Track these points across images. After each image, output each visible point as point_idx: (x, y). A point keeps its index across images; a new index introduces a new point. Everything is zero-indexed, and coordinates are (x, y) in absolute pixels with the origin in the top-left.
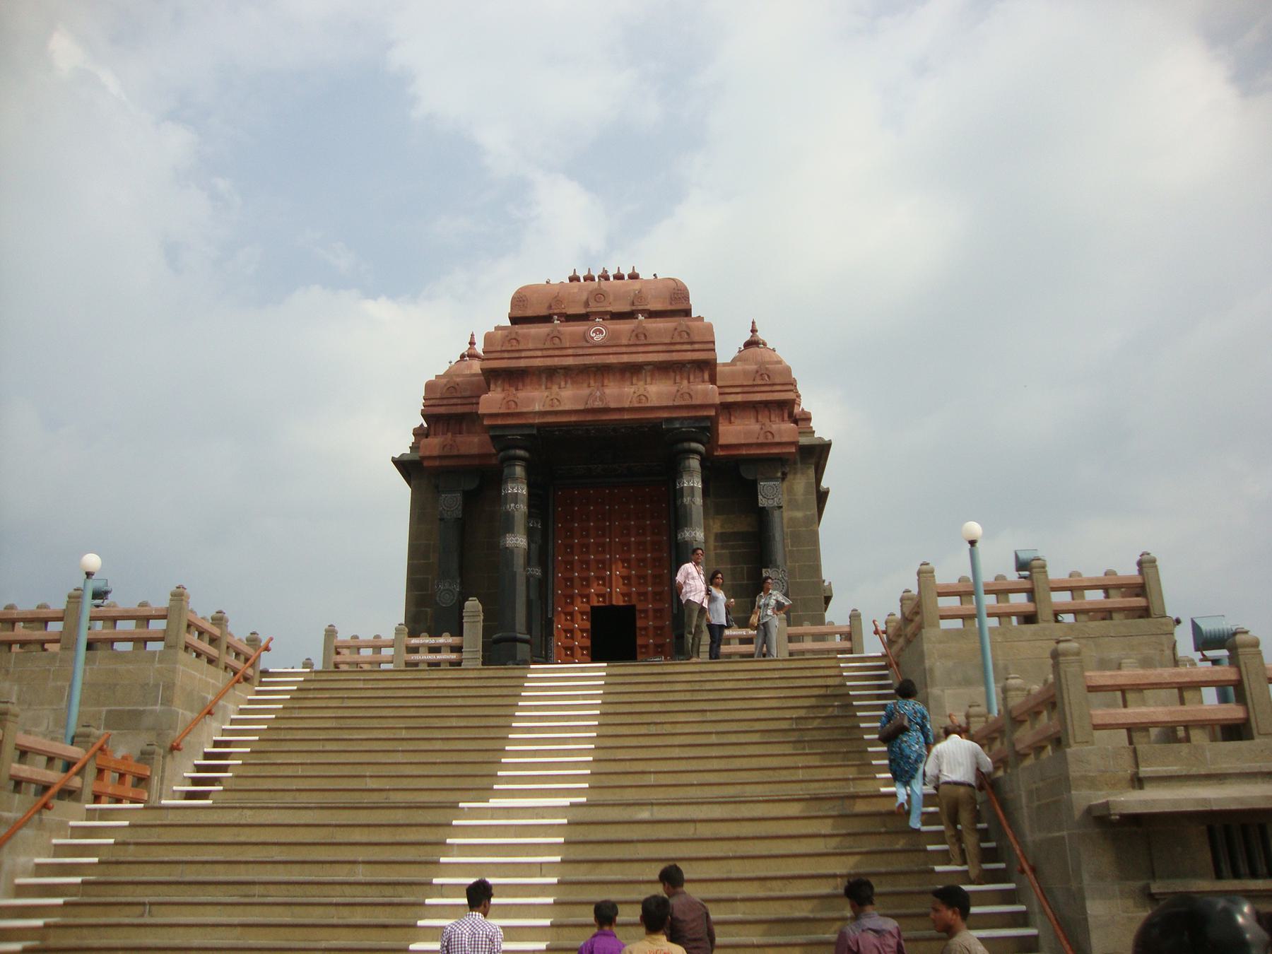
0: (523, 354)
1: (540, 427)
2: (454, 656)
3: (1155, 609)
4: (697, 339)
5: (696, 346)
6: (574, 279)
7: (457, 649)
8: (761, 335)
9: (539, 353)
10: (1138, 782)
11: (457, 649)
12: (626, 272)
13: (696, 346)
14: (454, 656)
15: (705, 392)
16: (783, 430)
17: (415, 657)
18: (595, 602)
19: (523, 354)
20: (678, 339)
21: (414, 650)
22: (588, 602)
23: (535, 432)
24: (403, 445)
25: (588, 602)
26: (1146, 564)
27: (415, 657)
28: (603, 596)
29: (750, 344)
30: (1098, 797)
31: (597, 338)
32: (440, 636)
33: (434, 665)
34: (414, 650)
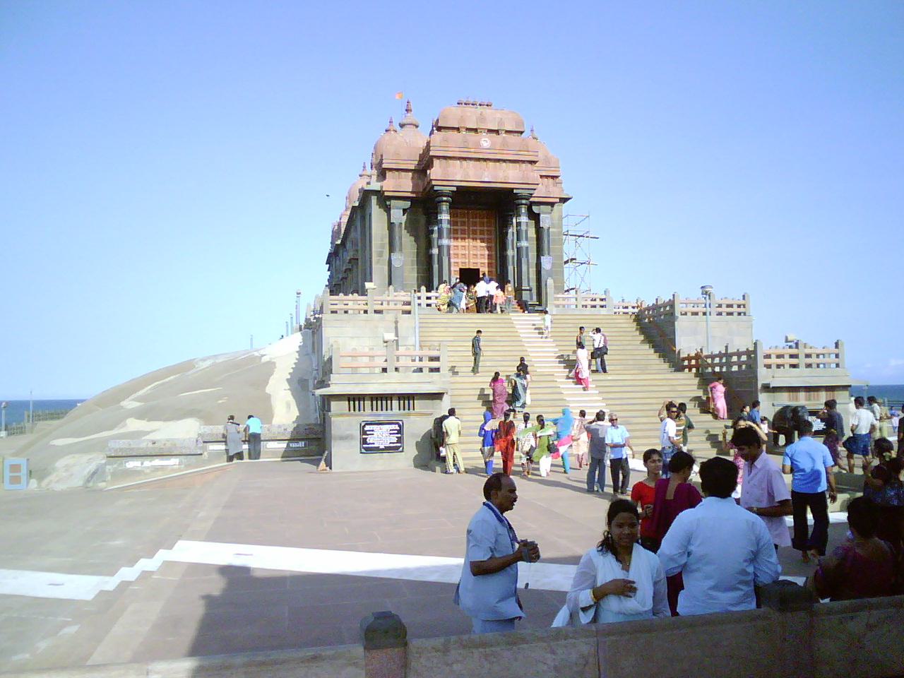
0: (451, 149)
1: (457, 187)
3: (747, 314)
4: (530, 150)
5: (531, 153)
9: (458, 149)
13: (531, 153)
15: (532, 174)
16: (555, 192)
19: (451, 149)
20: (521, 149)
21: (428, 298)
22: (458, 266)
23: (455, 189)
25: (458, 266)
28: (465, 263)
30: (766, 382)
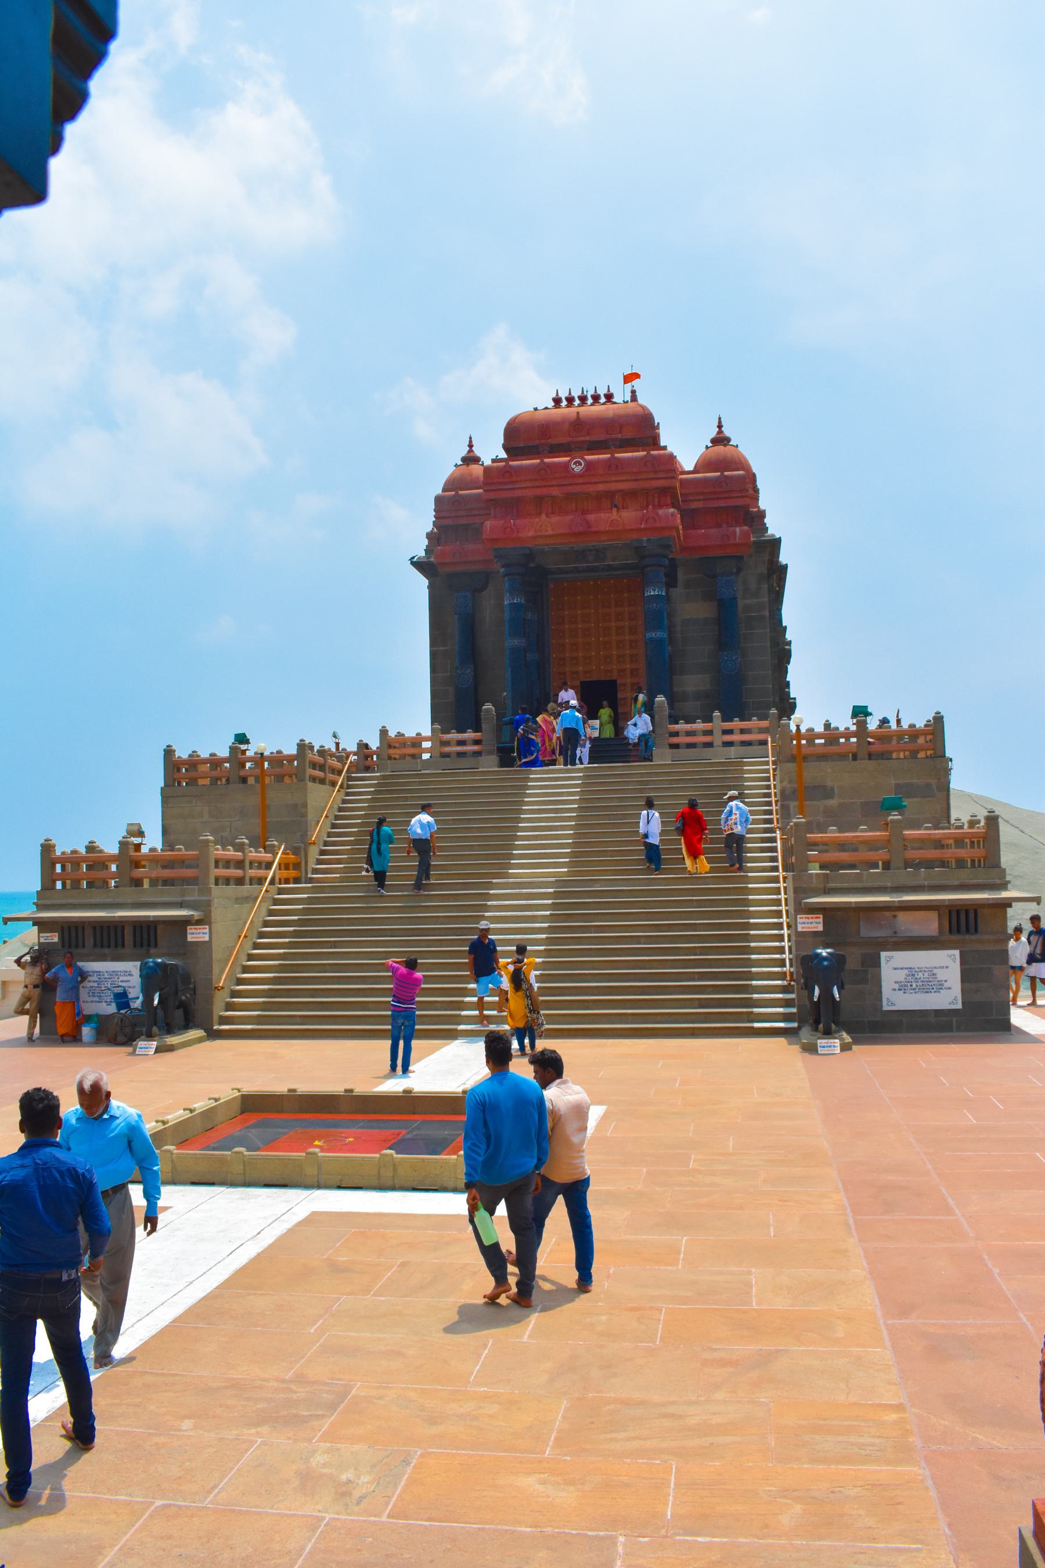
2: (476, 748)
6: (557, 401)
7: (477, 742)
8: (727, 431)
10: (827, 892)
11: (477, 742)
12: (602, 392)
14: (476, 748)
17: (447, 749)
18: (582, 679)
24: (419, 548)
26: (939, 719)
27: (447, 749)
29: (715, 441)
31: (577, 469)
32: (465, 732)
33: (461, 755)
34: (447, 743)
